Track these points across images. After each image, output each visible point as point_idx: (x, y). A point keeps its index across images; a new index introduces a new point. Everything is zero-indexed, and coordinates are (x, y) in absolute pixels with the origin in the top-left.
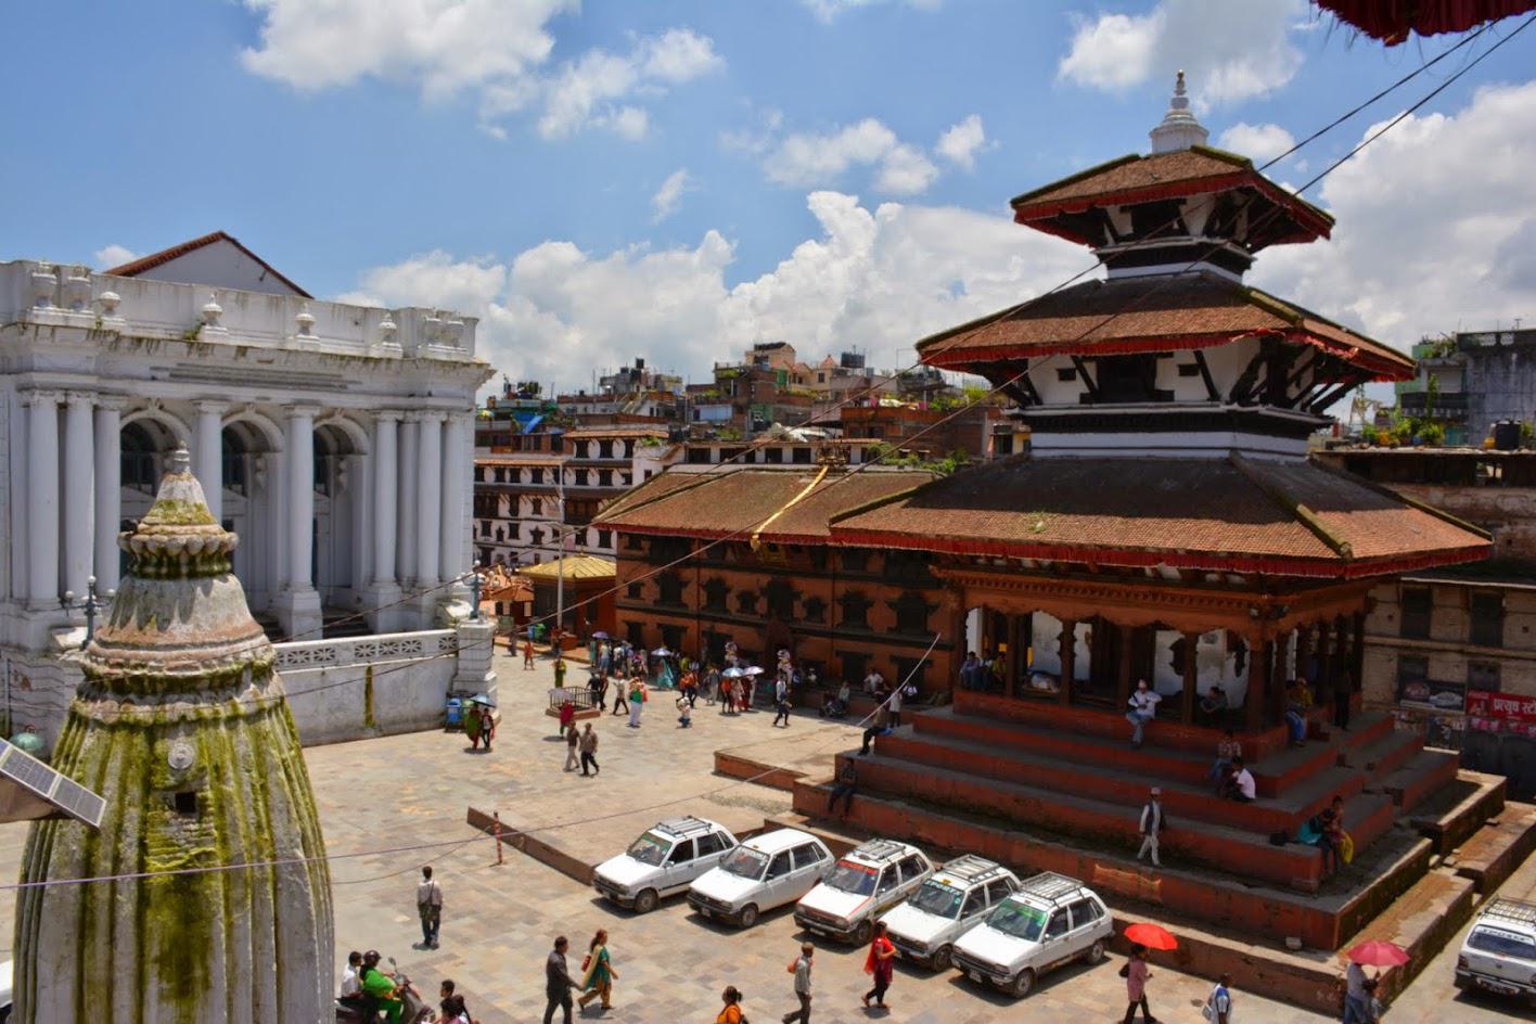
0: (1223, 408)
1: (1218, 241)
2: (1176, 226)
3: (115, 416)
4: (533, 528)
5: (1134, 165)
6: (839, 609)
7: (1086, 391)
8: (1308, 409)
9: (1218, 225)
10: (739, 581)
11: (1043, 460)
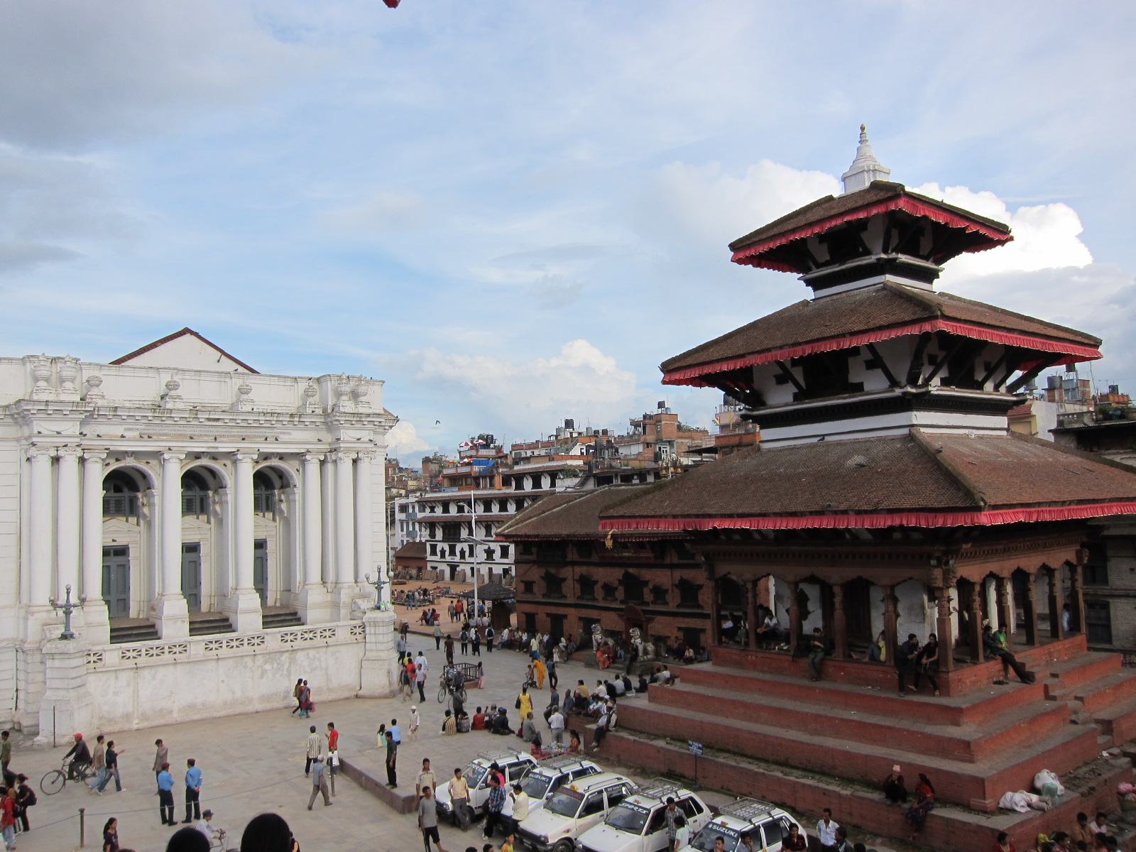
0: (898, 392)
1: (894, 255)
2: (861, 250)
3: (99, 466)
4: (486, 547)
5: (831, 203)
6: (677, 592)
7: (796, 390)
8: (1003, 389)
9: (894, 241)
10: (604, 575)
11: (769, 450)
